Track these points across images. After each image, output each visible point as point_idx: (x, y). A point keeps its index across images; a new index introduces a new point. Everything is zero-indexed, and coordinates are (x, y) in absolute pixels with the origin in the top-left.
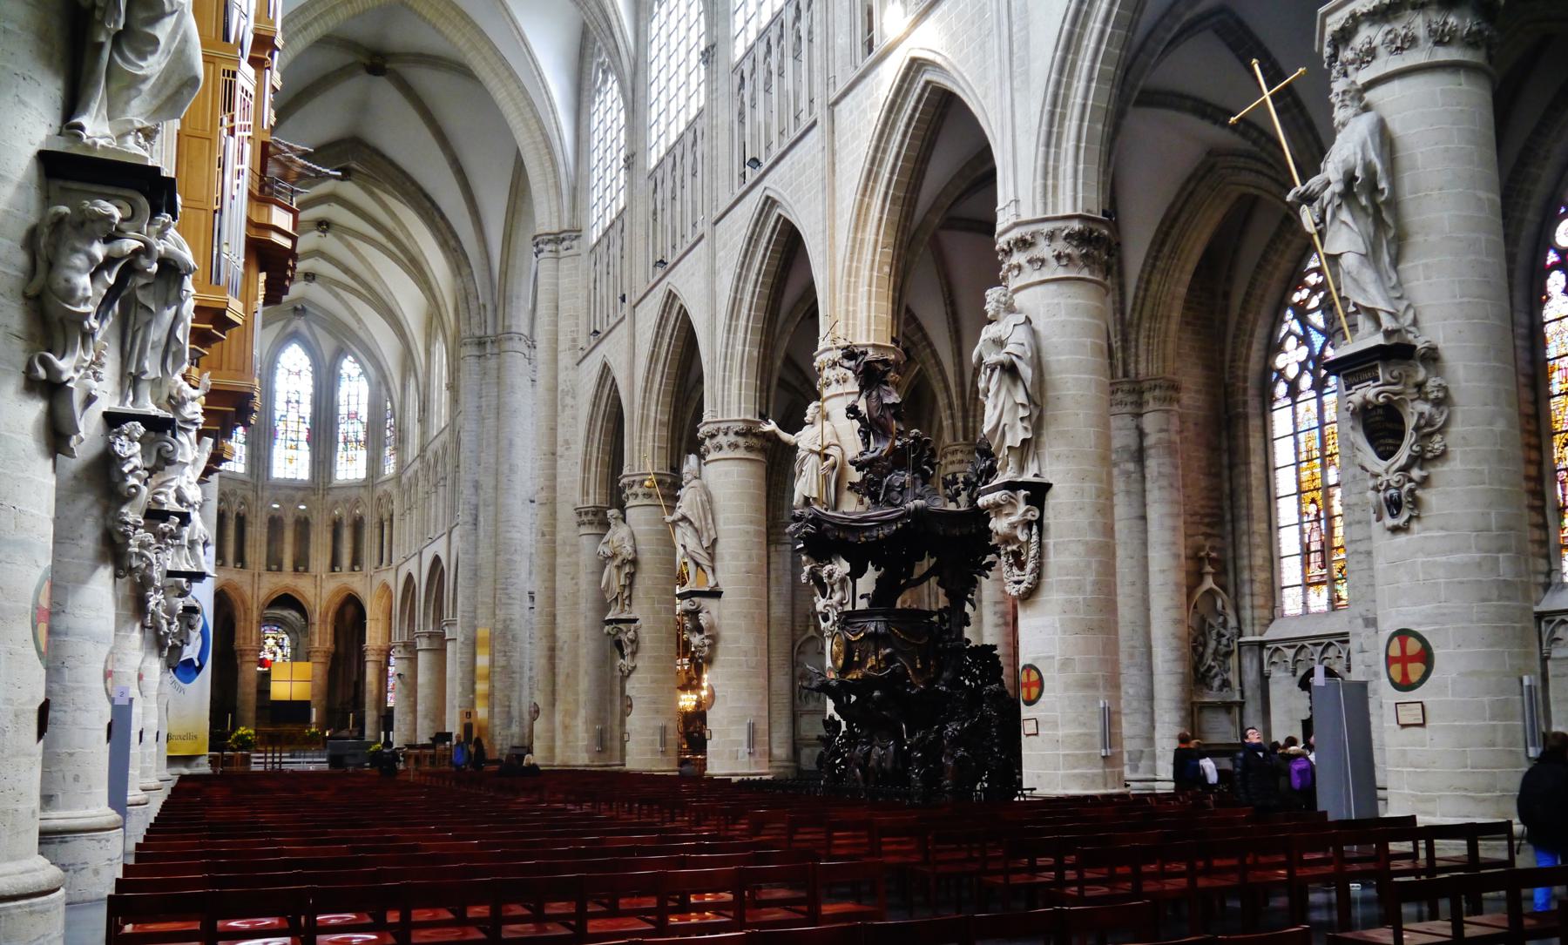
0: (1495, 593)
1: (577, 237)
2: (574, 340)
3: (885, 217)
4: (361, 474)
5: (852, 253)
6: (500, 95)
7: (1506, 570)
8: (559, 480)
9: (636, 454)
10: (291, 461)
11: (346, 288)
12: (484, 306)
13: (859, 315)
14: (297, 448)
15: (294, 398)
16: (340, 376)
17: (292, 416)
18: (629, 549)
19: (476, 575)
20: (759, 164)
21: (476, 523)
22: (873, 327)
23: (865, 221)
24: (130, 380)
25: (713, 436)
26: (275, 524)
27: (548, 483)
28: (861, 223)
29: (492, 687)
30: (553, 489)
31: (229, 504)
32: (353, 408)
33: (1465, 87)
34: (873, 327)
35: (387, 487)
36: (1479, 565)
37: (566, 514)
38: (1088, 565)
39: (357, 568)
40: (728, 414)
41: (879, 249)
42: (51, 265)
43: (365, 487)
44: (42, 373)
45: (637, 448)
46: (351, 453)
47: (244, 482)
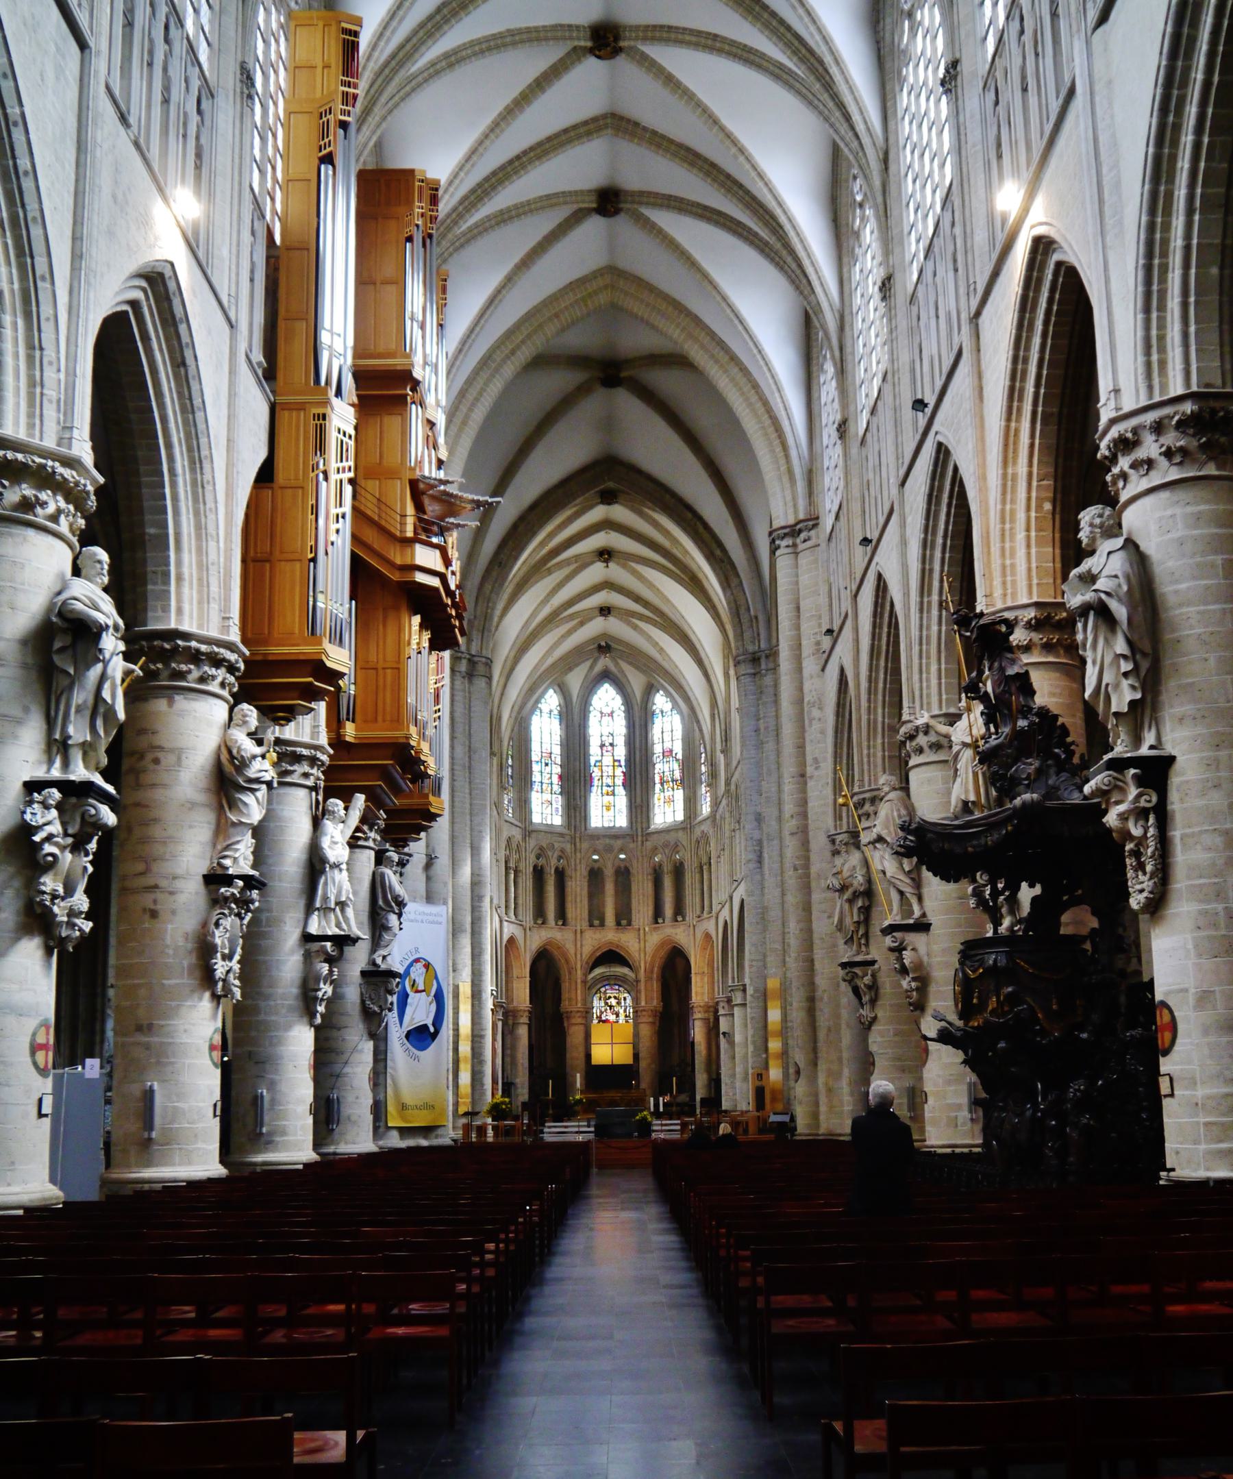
2: (818, 643)
3: (1037, 441)
4: (680, 816)
5: (1004, 493)
6: (723, 383)
8: (810, 805)
9: (866, 767)
10: (608, 808)
11: (641, 617)
12: (756, 618)
13: (1018, 569)
15: (608, 741)
16: (653, 713)
17: (608, 760)
18: (860, 879)
19: (763, 918)
20: (926, 405)
21: (760, 861)
22: (1035, 581)
23: (1015, 451)
24: (58, 746)
25: (912, 737)
26: (595, 875)
27: (797, 809)
28: (1011, 455)
29: (785, 1045)
30: (804, 815)
31: (547, 858)
32: (668, 745)
34: (1035, 581)
35: (705, 827)
37: (819, 842)
39: (680, 918)
41: (1035, 483)
43: (684, 829)
45: (865, 760)
46: (668, 793)
47: (562, 835)
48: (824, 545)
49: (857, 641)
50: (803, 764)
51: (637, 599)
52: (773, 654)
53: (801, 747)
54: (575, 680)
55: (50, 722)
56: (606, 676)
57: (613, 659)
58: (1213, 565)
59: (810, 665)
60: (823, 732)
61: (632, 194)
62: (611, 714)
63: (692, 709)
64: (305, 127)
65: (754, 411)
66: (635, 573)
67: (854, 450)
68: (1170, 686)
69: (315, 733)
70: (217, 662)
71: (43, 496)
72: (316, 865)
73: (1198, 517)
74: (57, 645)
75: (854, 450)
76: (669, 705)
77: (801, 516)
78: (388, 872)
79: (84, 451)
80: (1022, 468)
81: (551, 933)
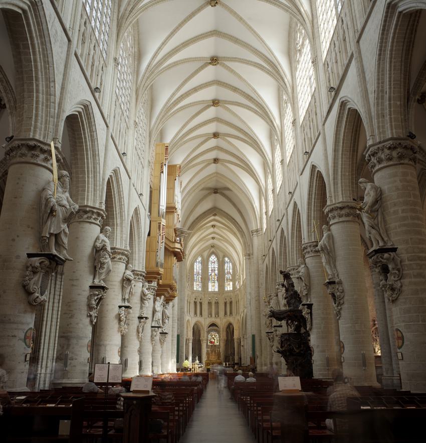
4: (231, 289)
14: (214, 283)
17: (213, 274)
21: (250, 304)
24: (124, 300)
26: (210, 303)
30: (259, 296)
37: (262, 302)
42: (90, 300)
47: (201, 293)
54: (206, 254)
55: (122, 296)
56: (213, 253)
59: (260, 262)
61: (221, 160)
62: (214, 262)
64: (158, 166)
68: (313, 291)
70: (141, 275)
76: (228, 261)
77: (259, 228)
78: (166, 310)
79: (128, 248)
81: (198, 318)
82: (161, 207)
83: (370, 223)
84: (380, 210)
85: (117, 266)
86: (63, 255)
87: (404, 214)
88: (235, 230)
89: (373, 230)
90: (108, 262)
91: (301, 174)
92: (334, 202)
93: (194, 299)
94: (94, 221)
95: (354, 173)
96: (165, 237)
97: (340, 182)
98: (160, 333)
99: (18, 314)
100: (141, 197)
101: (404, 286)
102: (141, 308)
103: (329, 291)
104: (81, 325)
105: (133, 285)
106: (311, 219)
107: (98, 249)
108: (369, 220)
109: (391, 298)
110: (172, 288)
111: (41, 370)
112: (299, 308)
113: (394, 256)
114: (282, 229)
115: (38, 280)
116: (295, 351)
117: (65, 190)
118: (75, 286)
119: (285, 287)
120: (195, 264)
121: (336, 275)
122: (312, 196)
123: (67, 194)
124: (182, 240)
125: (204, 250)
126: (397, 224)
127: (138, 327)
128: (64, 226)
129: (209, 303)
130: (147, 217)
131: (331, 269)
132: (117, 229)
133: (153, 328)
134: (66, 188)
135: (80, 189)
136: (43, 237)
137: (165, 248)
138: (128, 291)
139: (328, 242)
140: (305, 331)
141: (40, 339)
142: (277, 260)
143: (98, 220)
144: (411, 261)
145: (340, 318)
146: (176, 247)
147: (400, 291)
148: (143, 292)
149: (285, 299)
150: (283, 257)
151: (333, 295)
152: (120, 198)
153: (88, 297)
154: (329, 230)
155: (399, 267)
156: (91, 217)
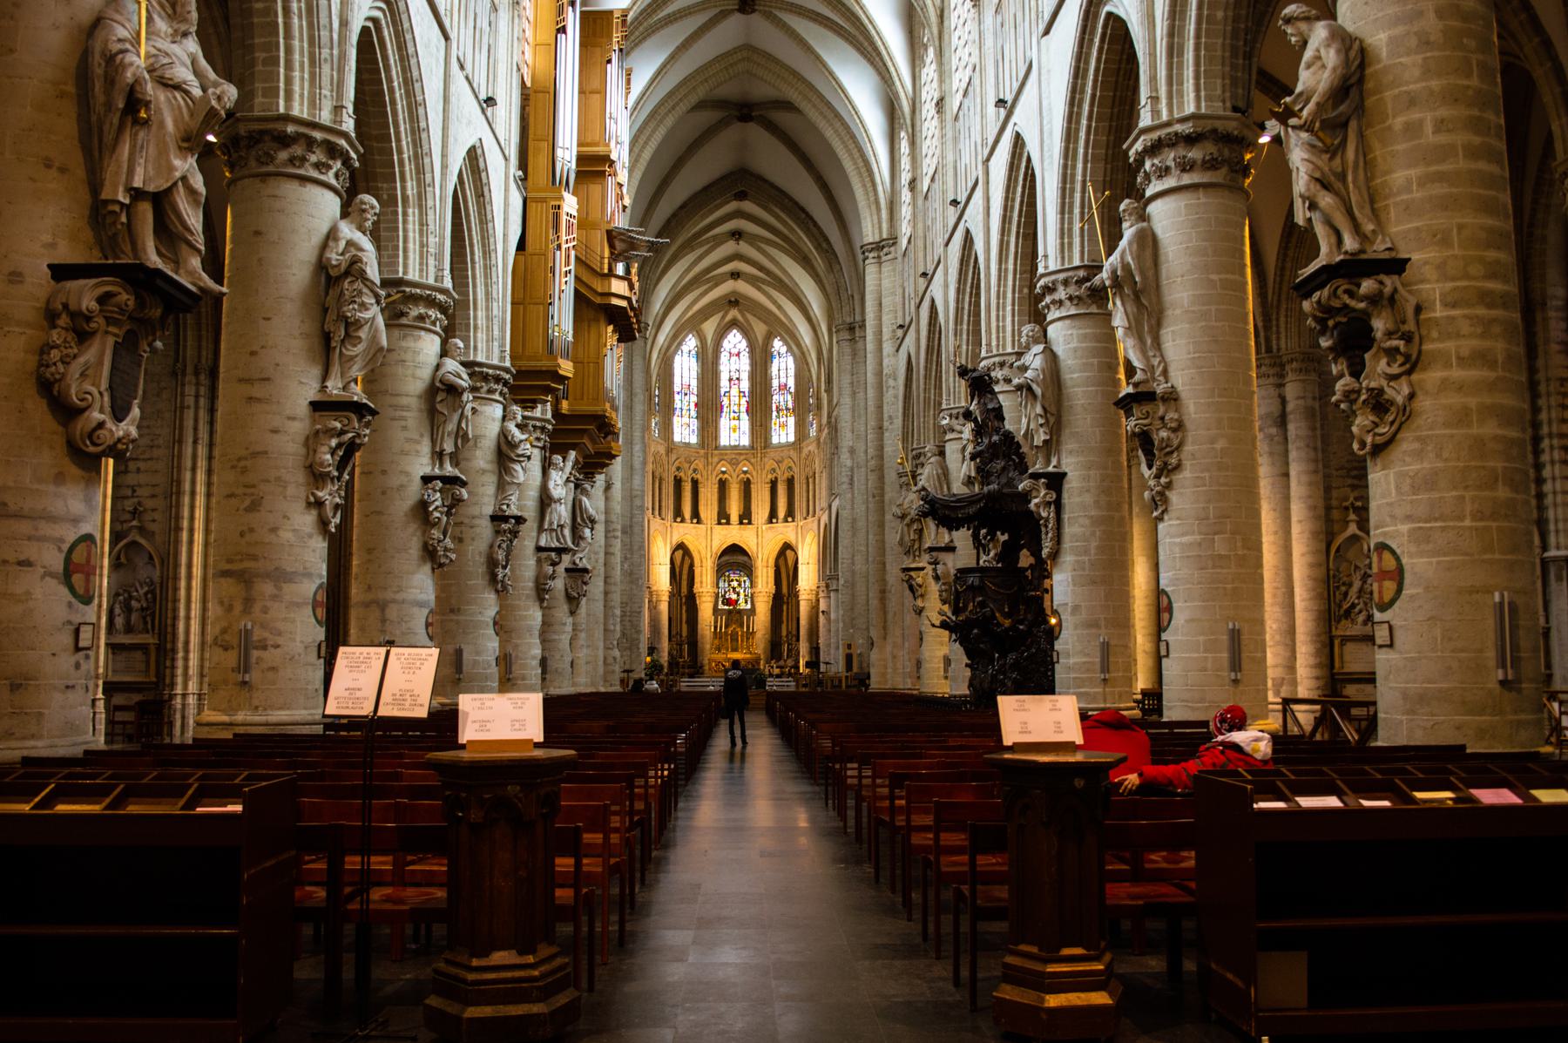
0: (1210, 563)
1: (894, 244)
4: (792, 438)
7: (1220, 547)
11: (764, 281)
17: (734, 391)
21: (851, 483)
24: (438, 456)
26: (723, 486)
32: (783, 380)
33: (1203, 200)
36: (1200, 544)
37: (891, 476)
38: (1093, 533)
40: (959, 402)
42: (315, 451)
44: (312, 499)
48: (900, 259)
49: (918, 339)
50: (880, 419)
51: (761, 268)
52: (863, 326)
53: (880, 407)
54: (710, 327)
55: (433, 442)
56: (734, 324)
57: (740, 311)
58: (1092, 365)
59: (888, 348)
60: (896, 397)
62: (738, 355)
63: (803, 353)
65: (851, 155)
66: (759, 249)
67: (920, 202)
68: (1066, 433)
69: (544, 412)
70: (498, 379)
71: (430, 313)
72: (545, 500)
73: (1085, 336)
74: (439, 399)
75: (920, 202)
76: (784, 349)
77: (885, 236)
78: (584, 499)
79: (448, 283)
80: (1011, 267)
82: (559, 152)
83: (1317, 167)
84: (1353, 125)
85: (412, 344)
86: (192, 273)
87: (1443, 139)
88: (809, 246)
89: (1324, 192)
90: (374, 318)
91: (1047, 32)
92: (1165, 117)
93: (674, 469)
94: (315, 174)
95: (1243, 12)
96: (576, 257)
97: (1190, 45)
98: (567, 570)
99: (36, 486)
100: (489, 111)
101: (1420, 396)
102: (502, 486)
103: (1130, 425)
104: (286, 535)
105: (469, 406)
106: (1072, 190)
107: (333, 273)
108: (1314, 159)
109: (1369, 440)
110: (604, 426)
111: (185, 686)
112: (1021, 487)
113: (1395, 290)
114: (968, 231)
115: (100, 363)
116: (999, 625)
117: (183, 27)
118: (259, 400)
119: (975, 420)
120: (677, 360)
121: (1158, 372)
122: (1080, 106)
123: (192, 45)
124: (634, 271)
125: (705, 314)
126: (1413, 173)
127: (491, 546)
128: (186, 165)
129: (721, 480)
130: (513, 186)
131: (1144, 352)
132: (405, 214)
133: (544, 555)
134: (185, 20)
135: (260, 55)
136: (106, 202)
137: (577, 293)
138: (451, 426)
139: (1139, 258)
140: (1031, 560)
141: (176, 589)
142: (947, 337)
143: (331, 173)
144: (1454, 305)
145: (1163, 512)
146: (614, 290)
147: (1407, 413)
148: (504, 434)
149: (973, 458)
150: (965, 327)
151: (1144, 440)
152: (415, 105)
153: (307, 438)
154: (1143, 217)
155: (1410, 326)
156: (304, 159)
